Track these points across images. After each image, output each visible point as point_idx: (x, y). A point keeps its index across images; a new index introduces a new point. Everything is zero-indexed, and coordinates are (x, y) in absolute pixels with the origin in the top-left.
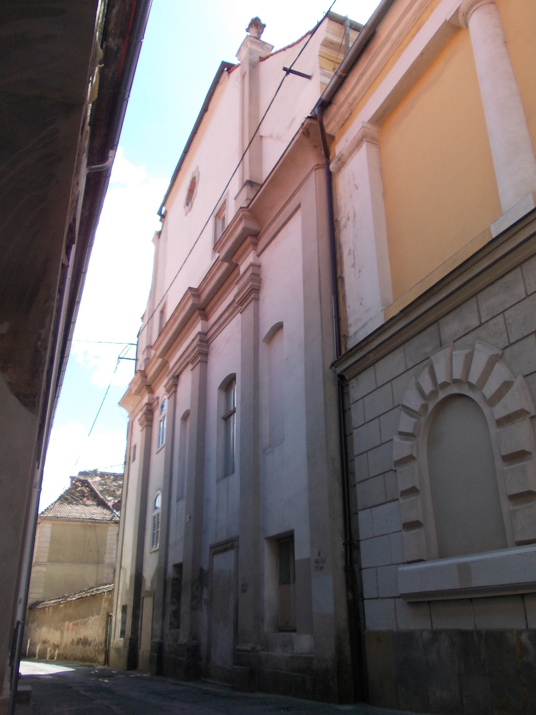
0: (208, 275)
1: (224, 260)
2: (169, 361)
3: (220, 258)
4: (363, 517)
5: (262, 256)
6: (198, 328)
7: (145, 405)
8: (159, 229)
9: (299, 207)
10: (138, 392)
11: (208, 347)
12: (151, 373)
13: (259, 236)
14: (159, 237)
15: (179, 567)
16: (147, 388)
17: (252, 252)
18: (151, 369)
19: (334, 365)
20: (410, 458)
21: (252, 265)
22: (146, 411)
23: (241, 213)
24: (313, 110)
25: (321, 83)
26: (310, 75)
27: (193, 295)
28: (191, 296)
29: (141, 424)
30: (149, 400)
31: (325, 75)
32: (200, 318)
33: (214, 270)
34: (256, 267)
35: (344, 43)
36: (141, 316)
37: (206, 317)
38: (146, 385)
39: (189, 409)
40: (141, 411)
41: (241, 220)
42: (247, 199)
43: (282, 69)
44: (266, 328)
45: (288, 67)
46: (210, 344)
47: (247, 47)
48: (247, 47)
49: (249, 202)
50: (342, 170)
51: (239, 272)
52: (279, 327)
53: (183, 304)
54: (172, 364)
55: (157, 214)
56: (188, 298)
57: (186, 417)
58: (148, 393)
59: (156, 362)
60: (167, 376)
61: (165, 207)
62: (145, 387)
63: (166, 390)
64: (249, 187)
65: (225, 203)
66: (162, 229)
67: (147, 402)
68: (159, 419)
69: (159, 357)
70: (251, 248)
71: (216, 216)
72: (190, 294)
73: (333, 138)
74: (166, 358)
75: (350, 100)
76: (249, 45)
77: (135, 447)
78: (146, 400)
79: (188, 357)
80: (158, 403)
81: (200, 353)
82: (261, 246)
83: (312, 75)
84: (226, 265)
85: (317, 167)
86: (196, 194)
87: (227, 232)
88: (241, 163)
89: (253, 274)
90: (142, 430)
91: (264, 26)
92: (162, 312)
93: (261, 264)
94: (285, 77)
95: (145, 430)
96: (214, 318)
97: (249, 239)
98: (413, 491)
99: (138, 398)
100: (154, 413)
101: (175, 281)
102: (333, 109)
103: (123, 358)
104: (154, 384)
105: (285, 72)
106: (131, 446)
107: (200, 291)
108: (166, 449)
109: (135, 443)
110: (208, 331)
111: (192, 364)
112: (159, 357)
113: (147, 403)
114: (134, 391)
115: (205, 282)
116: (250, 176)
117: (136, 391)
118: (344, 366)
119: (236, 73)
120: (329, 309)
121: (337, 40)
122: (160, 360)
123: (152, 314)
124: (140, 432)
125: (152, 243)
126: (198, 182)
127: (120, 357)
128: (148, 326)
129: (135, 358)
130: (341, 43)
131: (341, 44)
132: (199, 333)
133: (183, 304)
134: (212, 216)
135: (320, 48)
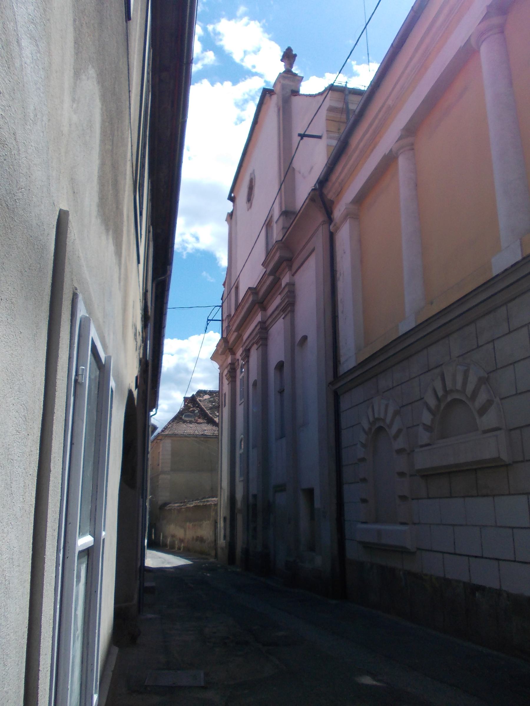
0: (261, 280)
1: (271, 273)
2: (243, 335)
3: (268, 272)
4: (346, 487)
5: (295, 276)
6: (259, 318)
7: (229, 365)
8: (230, 210)
9: (313, 250)
10: (223, 353)
11: (267, 333)
12: (232, 339)
13: (292, 260)
14: (231, 218)
15: (255, 496)
16: (229, 351)
17: (288, 272)
18: (231, 337)
19: (331, 383)
20: (363, 460)
21: (287, 284)
22: (230, 370)
23: (277, 246)
24: (315, 184)
25: (328, 145)
26: (320, 135)
27: (253, 293)
28: (251, 294)
29: (227, 379)
30: (231, 361)
31: (331, 138)
32: (259, 309)
33: (265, 278)
34: (291, 285)
35: (344, 107)
36: (223, 283)
37: (264, 309)
38: (229, 349)
39: (256, 379)
40: (227, 368)
41: (277, 250)
42: (283, 228)
43: (297, 135)
44: (298, 338)
45: (302, 133)
46: (268, 331)
47: (280, 82)
48: (280, 82)
49: (286, 230)
50: (338, 232)
51: (281, 284)
52: (305, 338)
53: (246, 298)
54: (245, 337)
55: (228, 199)
56: (250, 295)
57: (255, 384)
58: (231, 354)
59: (232, 335)
60: (242, 347)
61: (234, 194)
62: (228, 350)
63: (242, 359)
64: (285, 217)
65: (272, 216)
66: (233, 210)
67: (230, 362)
68: (240, 378)
69: (234, 332)
70: (287, 270)
71: (267, 225)
72: (250, 292)
73: (332, 202)
74: (240, 332)
75: (339, 180)
76: (282, 81)
77: (225, 394)
78: (229, 360)
79: (253, 338)
80: (238, 364)
81: (261, 338)
82: (295, 266)
83: (322, 135)
84: (271, 278)
85: (324, 223)
86: (254, 195)
87: (272, 252)
88: (280, 192)
89: (289, 291)
90: (228, 384)
91: (295, 56)
92: (237, 288)
93: (295, 282)
94: (301, 142)
95: (230, 385)
96: (271, 309)
97: (285, 264)
98: (364, 480)
99: (224, 356)
100: (236, 371)
101: (245, 263)
102: (330, 184)
103: (212, 320)
104: (234, 348)
105: (300, 138)
106: (223, 393)
107: (258, 289)
108: (244, 403)
109: (225, 392)
110: (267, 320)
111: (257, 345)
112: (234, 332)
113: (231, 363)
114: (220, 352)
115: (260, 284)
116: (285, 207)
117: (221, 352)
118: (339, 384)
119: (275, 98)
120: (330, 338)
121: (340, 105)
122: (236, 334)
123: (230, 290)
124: (228, 385)
125: (226, 222)
126: (255, 184)
127: (209, 319)
128: (228, 299)
129: (221, 319)
130: (342, 107)
131: (343, 108)
132: (259, 322)
133: (246, 298)
134: (264, 226)
135: (327, 113)
